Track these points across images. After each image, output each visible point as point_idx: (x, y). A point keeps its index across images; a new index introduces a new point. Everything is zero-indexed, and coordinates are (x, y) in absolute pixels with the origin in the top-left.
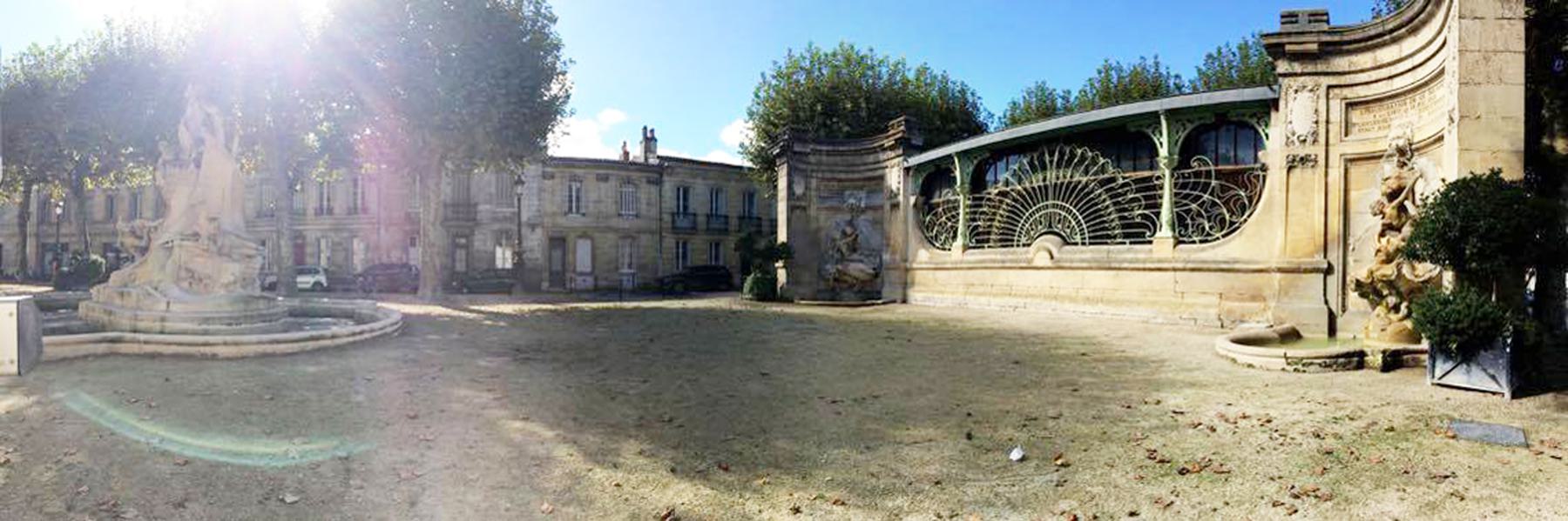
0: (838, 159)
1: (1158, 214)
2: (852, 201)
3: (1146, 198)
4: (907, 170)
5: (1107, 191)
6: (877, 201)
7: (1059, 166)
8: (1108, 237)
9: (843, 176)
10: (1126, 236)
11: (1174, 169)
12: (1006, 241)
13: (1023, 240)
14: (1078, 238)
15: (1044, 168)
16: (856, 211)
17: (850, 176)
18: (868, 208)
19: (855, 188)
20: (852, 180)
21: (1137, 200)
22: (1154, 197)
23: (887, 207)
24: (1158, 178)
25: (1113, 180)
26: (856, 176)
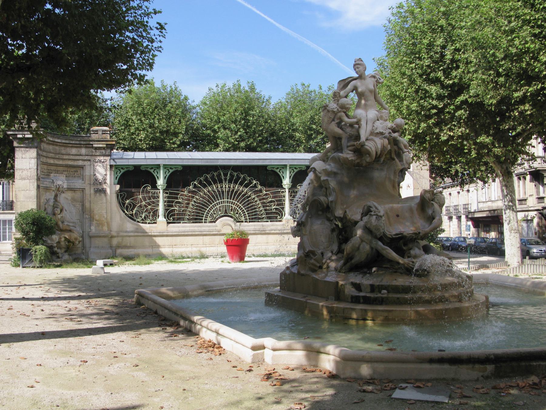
0: (51, 147)
1: (283, 208)
2: (60, 183)
3: (277, 201)
4: (111, 166)
5: (257, 196)
6: (78, 183)
7: (230, 182)
8: (260, 219)
9: (52, 161)
10: (269, 218)
11: (289, 189)
12: (197, 219)
13: (209, 219)
14: (243, 219)
15: (221, 182)
16: (59, 190)
17: (57, 162)
18: (70, 189)
19: (57, 172)
20: (57, 165)
21: (271, 202)
22: (280, 200)
23: (90, 191)
24: (283, 192)
25: (261, 191)
26: (61, 162)
